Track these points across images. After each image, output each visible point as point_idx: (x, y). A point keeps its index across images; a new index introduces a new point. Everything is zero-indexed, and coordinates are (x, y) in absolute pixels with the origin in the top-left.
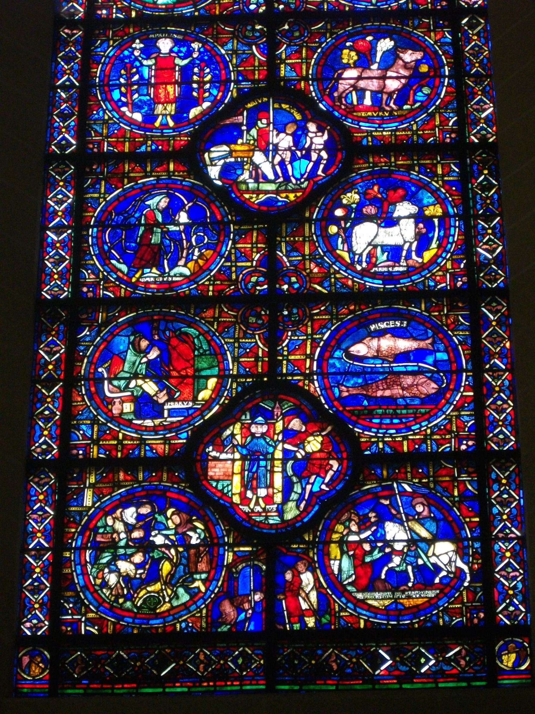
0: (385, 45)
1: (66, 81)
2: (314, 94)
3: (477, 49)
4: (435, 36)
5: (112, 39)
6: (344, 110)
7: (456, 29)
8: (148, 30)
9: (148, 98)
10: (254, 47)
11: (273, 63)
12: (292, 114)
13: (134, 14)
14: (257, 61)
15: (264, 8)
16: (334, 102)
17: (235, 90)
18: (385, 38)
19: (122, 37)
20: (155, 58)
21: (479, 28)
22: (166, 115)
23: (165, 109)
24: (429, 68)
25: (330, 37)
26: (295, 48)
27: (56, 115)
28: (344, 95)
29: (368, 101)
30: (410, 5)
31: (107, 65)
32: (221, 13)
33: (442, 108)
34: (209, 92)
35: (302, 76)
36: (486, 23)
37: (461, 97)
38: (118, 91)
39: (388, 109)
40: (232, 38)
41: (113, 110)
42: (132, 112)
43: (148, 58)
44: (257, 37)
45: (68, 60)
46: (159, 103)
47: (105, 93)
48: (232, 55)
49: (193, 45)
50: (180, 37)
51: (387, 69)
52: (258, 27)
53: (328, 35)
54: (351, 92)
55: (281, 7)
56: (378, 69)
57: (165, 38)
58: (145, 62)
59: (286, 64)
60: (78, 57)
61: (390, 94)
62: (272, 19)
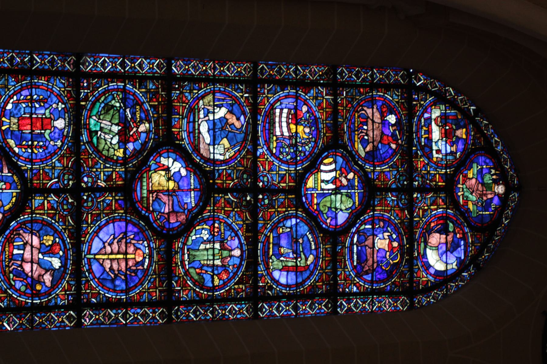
0: (56, 263)
1: (36, 60)
2: (22, 218)
3: (52, 320)
4: (62, 295)
5: (65, 90)
6: (10, 237)
7: (67, 308)
8: (71, 113)
9: (23, 113)
10: (57, 180)
11: (45, 192)
12: (9, 204)
13: (83, 103)
14: (47, 182)
15: (84, 186)
16: (16, 230)
17: (26, 168)
18: (61, 263)
19: (66, 96)
20: (50, 118)
21: (67, 323)
22: (10, 125)
23: (14, 124)
24: (39, 291)
25: (63, 228)
26: (55, 206)
27: (12, 55)
28: (21, 237)
29: (16, 252)
30: (84, 279)
31: (47, 87)
32: (82, 159)
33: (10, 298)
34: (26, 152)
35: (34, 210)
36: (70, 327)
37: (18, 309)
38: (28, 94)
39: (10, 265)
40: (63, 166)
41: (15, 92)
42: (12, 103)
43: (51, 113)
44: (63, 182)
45: (52, 62)
46: (19, 120)
47: (27, 86)
48: (52, 166)
49: (59, 141)
50: (65, 133)
51: (38, 264)
52: (71, 183)
53: (64, 227)
54: (23, 241)
55: (85, 198)
56: (39, 258)
57: (65, 124)
58: (48, 111)
59: (44, 200)
60: (53, 68)
61: (21, 266)
62: (76, 191)
